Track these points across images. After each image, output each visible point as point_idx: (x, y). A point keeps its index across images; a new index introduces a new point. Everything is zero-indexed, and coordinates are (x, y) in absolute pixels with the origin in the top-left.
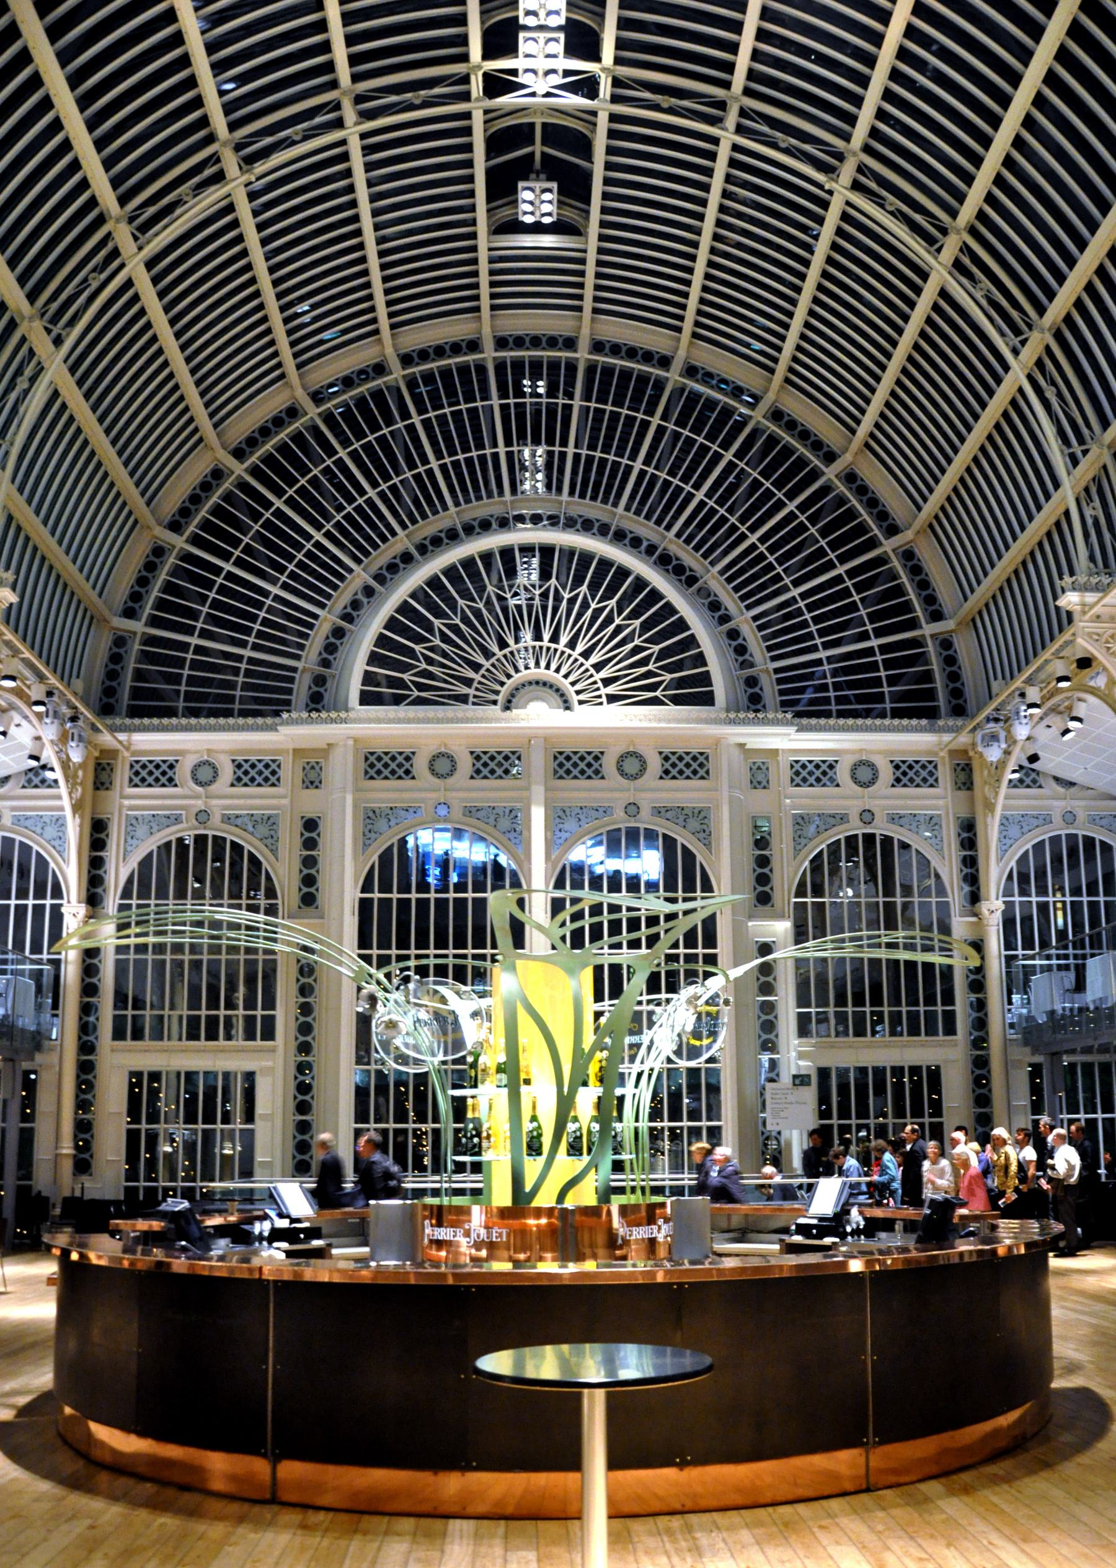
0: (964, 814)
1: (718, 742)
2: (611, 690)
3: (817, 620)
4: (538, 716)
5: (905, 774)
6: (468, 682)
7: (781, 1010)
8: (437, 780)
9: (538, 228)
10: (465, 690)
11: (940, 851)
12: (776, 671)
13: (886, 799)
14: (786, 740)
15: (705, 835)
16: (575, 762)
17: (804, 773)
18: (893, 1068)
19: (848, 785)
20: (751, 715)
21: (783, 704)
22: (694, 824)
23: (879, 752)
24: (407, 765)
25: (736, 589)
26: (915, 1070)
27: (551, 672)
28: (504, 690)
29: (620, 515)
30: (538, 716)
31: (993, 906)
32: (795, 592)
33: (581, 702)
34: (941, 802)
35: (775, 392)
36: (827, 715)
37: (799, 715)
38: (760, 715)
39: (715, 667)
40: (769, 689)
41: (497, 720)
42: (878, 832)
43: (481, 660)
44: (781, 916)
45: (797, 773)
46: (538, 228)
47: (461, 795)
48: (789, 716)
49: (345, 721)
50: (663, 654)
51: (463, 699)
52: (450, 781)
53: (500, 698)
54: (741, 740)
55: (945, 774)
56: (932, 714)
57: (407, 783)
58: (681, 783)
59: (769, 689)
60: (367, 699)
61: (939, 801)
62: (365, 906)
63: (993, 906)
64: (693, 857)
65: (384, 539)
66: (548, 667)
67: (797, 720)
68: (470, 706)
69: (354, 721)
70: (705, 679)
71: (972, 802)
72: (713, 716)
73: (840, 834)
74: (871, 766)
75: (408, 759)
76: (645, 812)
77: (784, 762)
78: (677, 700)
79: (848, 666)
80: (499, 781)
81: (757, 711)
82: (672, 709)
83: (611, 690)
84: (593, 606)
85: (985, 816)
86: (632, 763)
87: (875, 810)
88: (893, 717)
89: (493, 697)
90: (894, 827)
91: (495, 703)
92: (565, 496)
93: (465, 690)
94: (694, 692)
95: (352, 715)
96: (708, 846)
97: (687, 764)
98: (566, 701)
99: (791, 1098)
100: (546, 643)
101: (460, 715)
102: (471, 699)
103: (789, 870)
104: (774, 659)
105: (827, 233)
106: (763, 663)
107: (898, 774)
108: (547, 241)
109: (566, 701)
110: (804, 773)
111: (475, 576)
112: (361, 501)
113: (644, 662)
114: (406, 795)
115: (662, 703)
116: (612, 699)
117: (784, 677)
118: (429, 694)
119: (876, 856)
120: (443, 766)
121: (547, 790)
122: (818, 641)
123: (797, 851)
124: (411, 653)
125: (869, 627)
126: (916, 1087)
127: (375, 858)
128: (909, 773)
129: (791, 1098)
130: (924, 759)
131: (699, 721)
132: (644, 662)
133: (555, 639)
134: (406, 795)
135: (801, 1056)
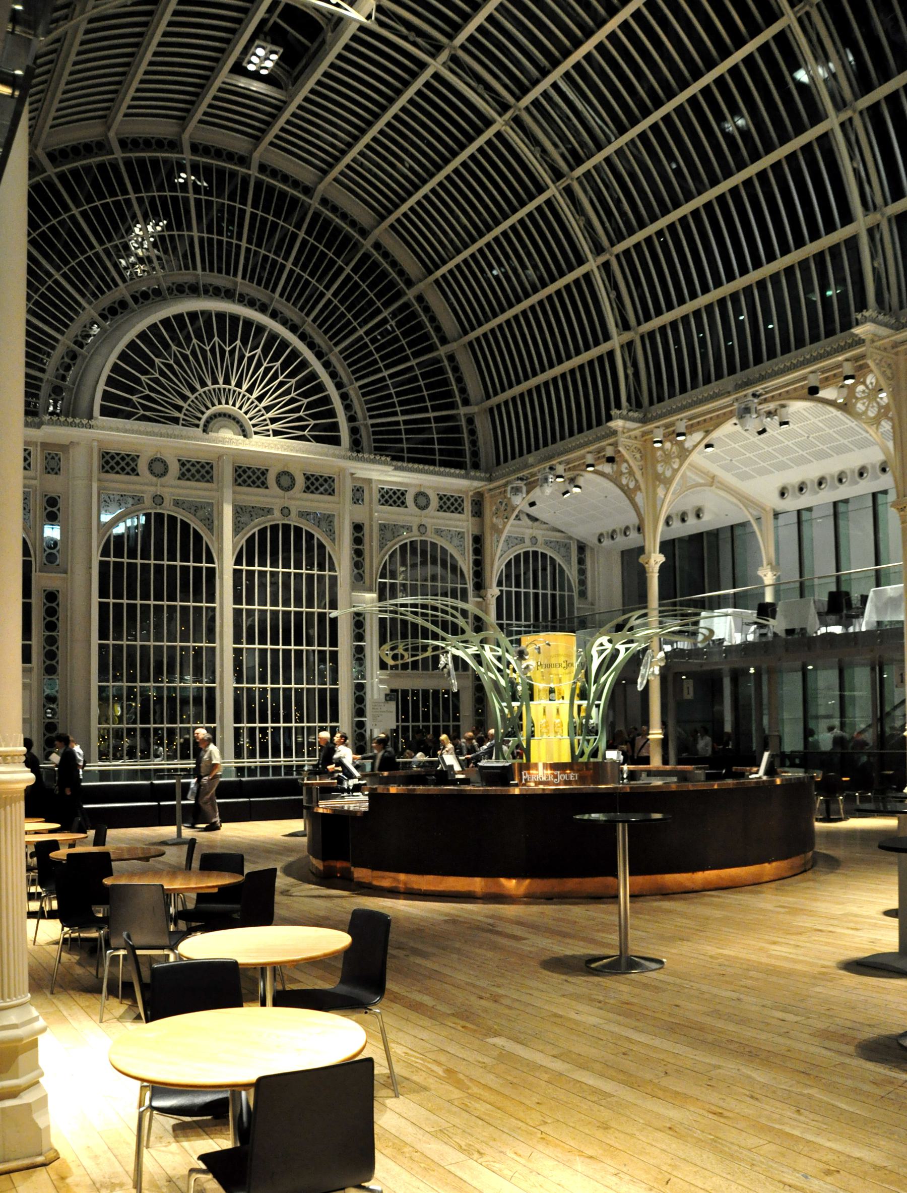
0: (476, 533)
1: (342, 471)
2: (275, 426)
3: (398, 394)
4: (227, 439)
5: (258, 478)
6: (179, 408)
7: (367, 652)
8: (155, 479)
9: (255, 76)
10: (176, 414)
11: (463, 554)
12: (373, 426)
13: (434, 518)
14: (384, 474)
15: (331, 533)
16: (250, 475)
17: (112, 463)
18: (413, 691)
19: (274, 489)
20: (355, 454)
21: (376, 449)
22: (324, 524)
23: (430, 488)
24: (133, 465)
25: (350, 365)
26: (415, 693)
27: (230, 406)
28: (204, 417)
29: (277, 302)
30: (227, 439)
31: (493, 591)
32: (386, 373)
33: (256, 433)
34: (465, 524)
35: (381, 233)
36: (432, 463)
37: (394, 458)
38: (360, 455)
39: (341, 418)
40: (365, 437)
41: (195, 439)
42: (166, 512)
43: (188, 393)
44: (370, 590)
45: (107, 462)
46: (255, 76)
47: (171, 490)
48: (389, 459)
49: (91, 427)
50: (309, 406)
51: (176, 421)
52: (164, 479)
53: (202, 423)
54: (353, 471)
55: (468, 506)
56: (460, 465)
57: (133, 478)
58: (193, 484)
59: (365, 437)
60: (105, 412)
61: (463, 523)
62: (103, 566)
63: (493, 591)
64: (324, 547)
65: (109, 288)
66: (234, 405)
67: (395, 463)
68: (180, 427)
69: (98, 428)
70: (335, 427)
71: (482, 525)
72: (337, 452)
73: (520, 550)
74: (164, 462)
75: (133, 460)
76: (294, 513)
77: (375, 487)
78: (318, 439)
79: (415, 428)
80: (128, 477)
81: (358, 452)
82: (314, 445)
83: (275, 426)
84: (265, 365)
85: (492, 535)
86: (286, 480)
87: (429, 526)
88: (440, 466)
89: (197, 422)
90: (177, 509)
91: (197, 426)
92: (239, 279)
93: (176, 414)
94: (327, 436)
95: (92, 422)
96: (211, 529)
97: (319, 483)
98: (243, 431)
99: (384, 709)
100: (232, 387)
101: (170, 432)
102: (181, 422)
103: (375, 559)
104: (371, 417)
105: (826, 242)
106: (365, 422)
107: (263, 478)
108: (256, 86)
109: (243, 431)
110: (112, 463)
111: (183, 326)
112: (90, 253)
113: (297, 410)
114: (132, 487)
115: (309, 441)
116: (276, 433)
117: (377, 430)
118: (158, 413)
119: (420, 553)
120: (158, 468)
121: (234, 492)
122: (398, 409)
123: (381, 547)
124: (138, 381)
125: (428, 404)
126: (415, 704)
127: (243, 541)
128: (450, 504)
129: (384, 709)
130: (456, 495)
131: (334, 456)
132: (297, 410)
133: (239, 385)
134: (132, 487)
135: (381, 682)
